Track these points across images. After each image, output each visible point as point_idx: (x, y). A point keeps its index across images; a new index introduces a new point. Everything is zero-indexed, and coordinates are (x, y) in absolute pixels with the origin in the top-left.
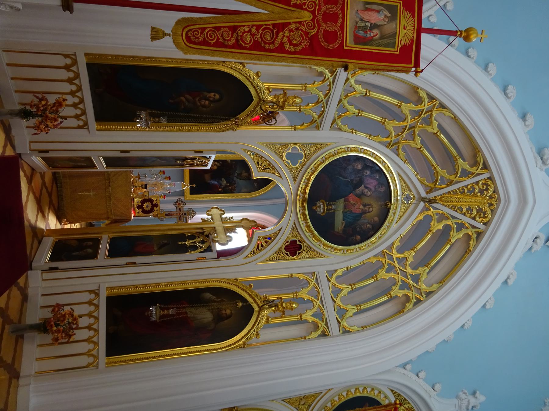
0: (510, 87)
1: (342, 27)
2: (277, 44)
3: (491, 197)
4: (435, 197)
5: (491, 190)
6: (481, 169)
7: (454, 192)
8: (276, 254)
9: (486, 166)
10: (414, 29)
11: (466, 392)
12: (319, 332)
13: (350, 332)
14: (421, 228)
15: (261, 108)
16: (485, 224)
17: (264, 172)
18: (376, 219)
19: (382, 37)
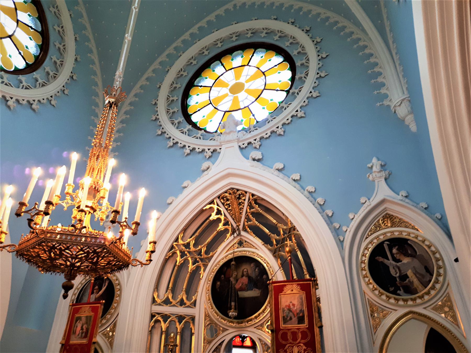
0: (167, 202)
3: (230, 194)
18: (252, 265)
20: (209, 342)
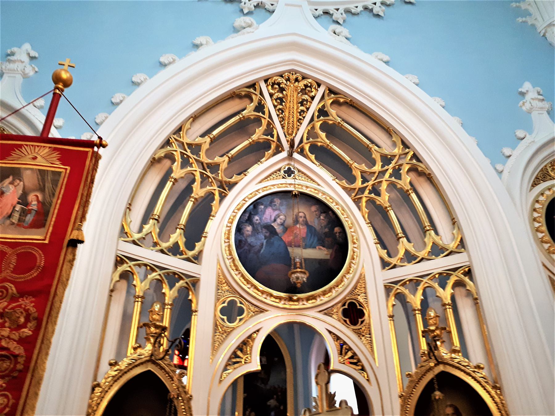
1: (13, 245)
2: (19, 350)
3: (288, 80)
4: (288, 141)
5: (280, 80)
6: (255, 90)
7: (282, 120)
8: (363, 338)
9: (253, 85)
10: (38, 146)
11: (521, 103)
12: (467, 279)
13: (462, 239)
14: (324, 156)
15: (161, 359)
16: (319, 85)
17: (250, 354)
19: (42, 189)
20: (228, 333)
